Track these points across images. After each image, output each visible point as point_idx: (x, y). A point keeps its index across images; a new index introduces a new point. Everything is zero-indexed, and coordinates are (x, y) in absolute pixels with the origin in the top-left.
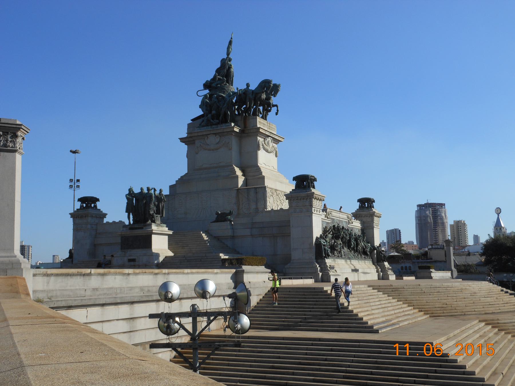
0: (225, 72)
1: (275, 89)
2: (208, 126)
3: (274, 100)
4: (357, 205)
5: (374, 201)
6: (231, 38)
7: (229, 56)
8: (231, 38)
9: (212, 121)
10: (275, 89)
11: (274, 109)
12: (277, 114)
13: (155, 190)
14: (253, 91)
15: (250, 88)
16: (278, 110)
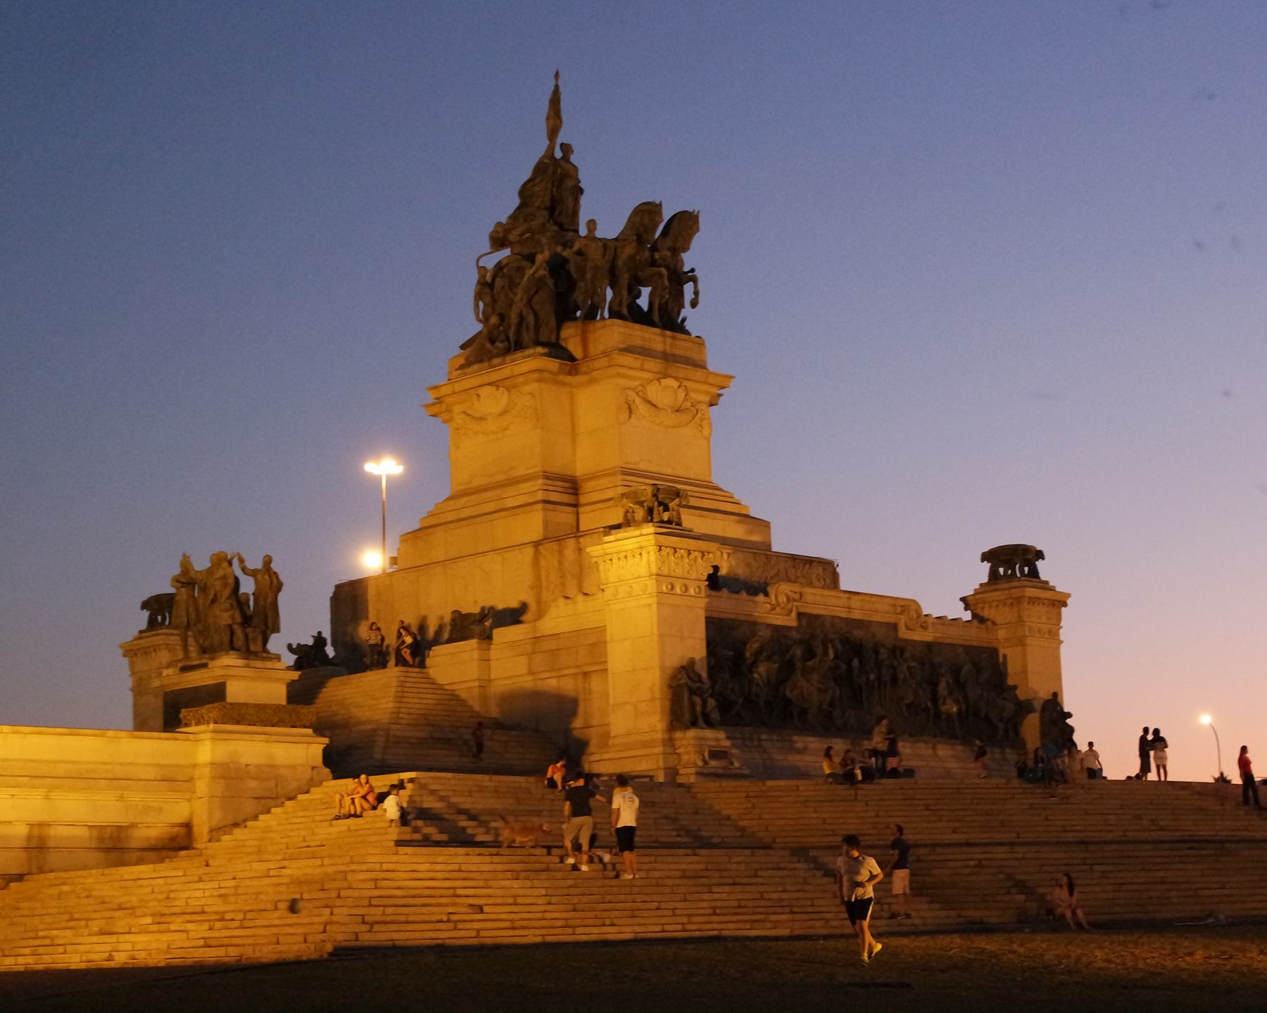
0: (553, 189)
1: (685, 224)
2: (481, 361)
3: (689, 260)
4: (982, 572)
5: (1040, 555)
6: (557, 87)
7: (562, 138)
8: (557, 87)
9: (488, 345)
10: (685, 224)
11: (688, 288)
12: (694, 304)
13: (242, 561)
14: (605, 243)
15: (599, 234)
16: (696, 293)
